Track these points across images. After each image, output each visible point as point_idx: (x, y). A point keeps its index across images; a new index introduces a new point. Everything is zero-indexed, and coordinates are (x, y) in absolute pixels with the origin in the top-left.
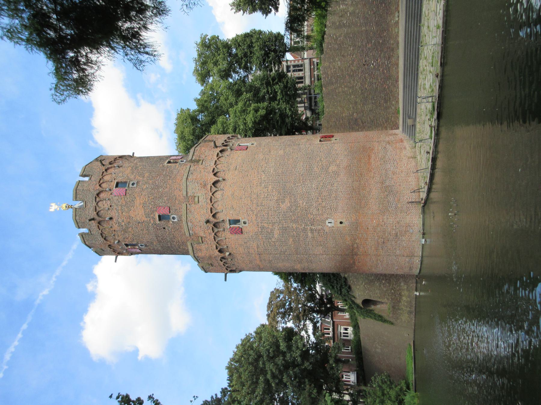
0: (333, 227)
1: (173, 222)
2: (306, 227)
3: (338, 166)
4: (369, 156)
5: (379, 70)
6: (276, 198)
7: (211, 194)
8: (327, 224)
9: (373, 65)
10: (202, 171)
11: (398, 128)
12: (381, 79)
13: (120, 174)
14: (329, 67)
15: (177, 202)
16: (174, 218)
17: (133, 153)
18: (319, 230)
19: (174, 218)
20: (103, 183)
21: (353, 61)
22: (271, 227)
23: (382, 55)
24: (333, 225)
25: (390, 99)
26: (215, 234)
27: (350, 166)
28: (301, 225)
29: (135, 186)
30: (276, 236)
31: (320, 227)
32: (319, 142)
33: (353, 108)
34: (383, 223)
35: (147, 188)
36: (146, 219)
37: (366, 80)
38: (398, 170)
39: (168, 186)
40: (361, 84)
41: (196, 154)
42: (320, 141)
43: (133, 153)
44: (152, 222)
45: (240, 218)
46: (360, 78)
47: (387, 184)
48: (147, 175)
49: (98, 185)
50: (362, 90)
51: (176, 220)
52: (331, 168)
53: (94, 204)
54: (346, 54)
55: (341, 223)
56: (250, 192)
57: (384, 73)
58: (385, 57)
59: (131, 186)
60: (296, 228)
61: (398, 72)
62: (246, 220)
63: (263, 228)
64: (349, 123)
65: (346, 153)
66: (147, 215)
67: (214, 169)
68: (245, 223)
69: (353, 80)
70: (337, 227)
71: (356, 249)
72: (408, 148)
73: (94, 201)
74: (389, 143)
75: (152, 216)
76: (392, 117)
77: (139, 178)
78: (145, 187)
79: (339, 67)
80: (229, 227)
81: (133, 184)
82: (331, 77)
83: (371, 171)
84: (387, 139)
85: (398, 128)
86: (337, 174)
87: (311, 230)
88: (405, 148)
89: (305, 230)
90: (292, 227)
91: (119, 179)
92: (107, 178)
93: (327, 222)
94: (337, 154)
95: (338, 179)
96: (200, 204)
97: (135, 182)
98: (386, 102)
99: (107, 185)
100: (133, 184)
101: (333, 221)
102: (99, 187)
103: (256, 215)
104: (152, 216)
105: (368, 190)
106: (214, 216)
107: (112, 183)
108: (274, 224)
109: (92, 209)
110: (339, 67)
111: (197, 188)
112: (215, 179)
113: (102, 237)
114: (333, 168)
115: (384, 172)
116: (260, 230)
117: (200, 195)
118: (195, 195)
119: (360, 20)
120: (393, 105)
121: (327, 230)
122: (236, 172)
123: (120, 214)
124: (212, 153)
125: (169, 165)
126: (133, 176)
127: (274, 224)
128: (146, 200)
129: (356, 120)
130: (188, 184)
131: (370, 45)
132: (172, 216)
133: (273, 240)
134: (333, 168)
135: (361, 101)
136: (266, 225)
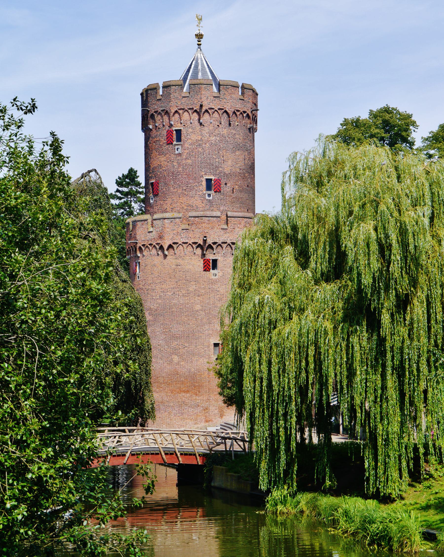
3: (178, 364)
4: (188, 391)
6: (152, 307)
10: (175, 232)
13: (190, 130)
15: (162, 202)
20: (179, 114)
27: (178, 374)
32: (213, 343)
35: (174, 166)
38: (172, 417)
39: (175, 190)
41: (197, 218)
47: (161, 407)
48: (189, 162)
49: (176, 109)
52: (176, 357)
59: (176, 147)
65: (193, 370)
67: (177, 243)
78: (175, 164)
83: (172, 392)
86: (171, 361)
91: (184, 133)
94: (192, 362)
95: (166, 364)
102: (173, 111)
103: (142, 289)
105: (157, 390)
107: (180, 125)
109: (156, 107)
112: (166, 247)
114: (176, 359)
115: (172, 404)
122: (174, 267)
124: (197, 236)
125: (204, 183)
128: (163, 168)
134: (176, 359)
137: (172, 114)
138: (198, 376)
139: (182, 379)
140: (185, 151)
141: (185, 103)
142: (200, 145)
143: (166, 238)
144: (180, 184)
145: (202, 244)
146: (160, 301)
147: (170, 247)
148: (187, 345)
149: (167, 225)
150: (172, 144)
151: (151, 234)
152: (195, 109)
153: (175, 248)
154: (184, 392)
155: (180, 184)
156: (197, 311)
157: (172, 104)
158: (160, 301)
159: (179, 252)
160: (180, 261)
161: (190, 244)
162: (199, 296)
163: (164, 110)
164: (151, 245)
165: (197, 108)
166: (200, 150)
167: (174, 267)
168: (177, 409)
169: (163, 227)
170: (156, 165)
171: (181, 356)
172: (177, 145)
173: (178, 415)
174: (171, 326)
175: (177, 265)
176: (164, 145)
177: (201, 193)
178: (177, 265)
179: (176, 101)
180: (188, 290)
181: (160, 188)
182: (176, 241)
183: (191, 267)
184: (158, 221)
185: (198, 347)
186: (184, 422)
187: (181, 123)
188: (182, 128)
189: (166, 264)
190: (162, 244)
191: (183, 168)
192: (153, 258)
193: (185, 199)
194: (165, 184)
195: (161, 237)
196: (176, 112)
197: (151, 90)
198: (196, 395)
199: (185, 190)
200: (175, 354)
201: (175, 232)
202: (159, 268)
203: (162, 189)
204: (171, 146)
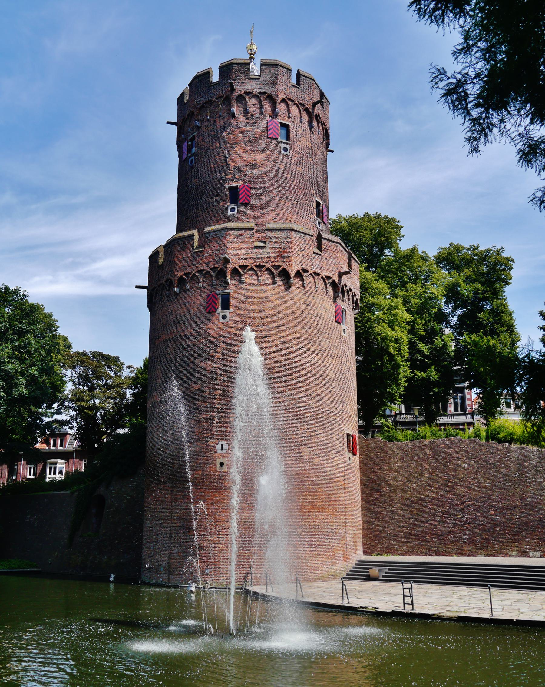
0: (216, 452)
1: (227, 208)
2: (216, 410)
3: (309, 461)
5: (454, 527)
7: (269, 266)
8: (221, 443)
9: (463, 517)
10: (305, 254)
11: (365, 553)
12: (440, 529)
14: (462, 451)
16: (233, 210)
17: (332, 151)
18: (211, 431)
19: (233, 210)
20: (288, 105)
21: (470, 488)
22: (217, 356)
23: (477, 531)
24: (219, 451)
25: (411, 542)
26: (207, 272)
28: (219, 403)
29: (283, 152)
30: (203, 364)
31: (215, 432)
32: (346, 432)
33: (397, 486)
34: (220, 528)
35: (279, 169)
36: (232, 168)
37: (440, 506)
40: (434, 498)
41: (331, 244)
42: (348, 435)
43: (332, 151)
44: (228, 177)
45: (231, 310)
46: (443, 497)
48: (299, 169)
49: (284, 97)
50: (424, 500)
51: (229, 212)
52: (306, 449)
53: (256, 91)
54: (480, 476)
55: (222, 464)
56: (271, 326)
57: (450, 533)
58: (474, 535)
59: (283, 146)
60: (215, 396)
61: (450, 555)
62: (228, 319)
63: (216, 345)
64: (374, 480)
65: (328, 473)
66: (237, 170)
68: (224, 317)
69: (439, 487)
70: (215, 459)
71: (181, 486)
72: (334, 568)
73: (260, 91)
74: (343, 539)
75: (237, 177)
76: (383, 544)
77: (295, 158)
78: (281, 166)
79: (460, 465)
80: (218, 292)
81: (285, 149)
82: (446, 453)
84: (349, 537)
85: (365, 553)
87: (212, 419)
88: (334, 564)
89: (212, 408)
90: (216, 390)
91: (292, 131)
92: (294, 110)
93: (224, 443)
94: (327, 459)
96: (254, 250)
97: (288, 153)
98: (405, 537)
99: (283, 111)
100: (285, 149)
101: (224, 451)
102: (281, 97)
104: (237, 177)
106: (235, 271)
107: (287, 118)
108: (222, 361)
109: (249, 87)
110: (460, 465)
111: (278, 245)
113: (206, 103)
114: (306, 452)
116: (212, 340)
117: (268, 249)
118: (267, 242)
119: (531, 497)
120: (400, 547)
121: (212, 442)
122: (301, 305)
123: (241, 130)
125: (315, 205)
126: (297, 149)
127: (222, 361)
129: (380, 491)
130: (285, 232)
131: (493, 513)
132: (236, 207)
133: (197, 360)
135: (408, 498)
136: (219, 349)
137: (279, 100)
138: (334, 484)
139: (316, 487)
140: (295, 155)
141: (294, 93)
142: (310, 154)
143: (293, 259)
144: (288, 195)
145: (337, 281)
146: (278, 357)
147: (298, 274)
148: (320, 431)
149: (294, 241)
150: (276, 139)
151: (260, 250)
152: (306, 106)
153: (305, 278)
154: (319, 509)
155: (288, 195)
156: (331, 380)
157: (280, 87)
158: (278, 357)
159: (309, 285)
160: (309, 299)
161: (322, 277)
162: (332, 357)
163: (265, 93)
164: (260, 267)
165: (309, 106)
166: (310, 160)
167: (301, 305)
168: (308, 538)
169: (289, 242)
170: (245, 163)
171: (312, 449)
172: (284, 143)
173: (310, 549)
174: (297, 399)
175: (307, 305)
176: (263, 138)
177: (312, 216)
178: (307, 305)
179: (285, 87)
180: (321, 346)
181: (253, 194)
182: (305, 268)
183: (323, 311)
184: (279, 232)
185: (334, 436)
186: (319, 562)
187: (289, 117)
188: (290, 124)
189: (288, 299)
190: (286, 267)
191: (292, 175)
192: (264, 287)
193: (295, 217)
194: (264, 190)
195: (283, 255)
196: (283, 100)
197: (238, 64)
198: (333, 514)
199: (295, 205)
200: (305, 445)
201: (305, 254)
202: (276, 304)
203: (257, 196)
204: (275, 141)
